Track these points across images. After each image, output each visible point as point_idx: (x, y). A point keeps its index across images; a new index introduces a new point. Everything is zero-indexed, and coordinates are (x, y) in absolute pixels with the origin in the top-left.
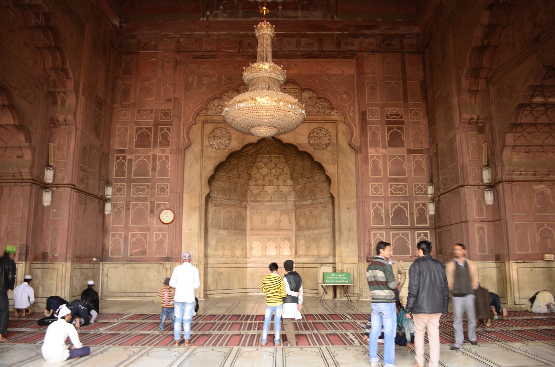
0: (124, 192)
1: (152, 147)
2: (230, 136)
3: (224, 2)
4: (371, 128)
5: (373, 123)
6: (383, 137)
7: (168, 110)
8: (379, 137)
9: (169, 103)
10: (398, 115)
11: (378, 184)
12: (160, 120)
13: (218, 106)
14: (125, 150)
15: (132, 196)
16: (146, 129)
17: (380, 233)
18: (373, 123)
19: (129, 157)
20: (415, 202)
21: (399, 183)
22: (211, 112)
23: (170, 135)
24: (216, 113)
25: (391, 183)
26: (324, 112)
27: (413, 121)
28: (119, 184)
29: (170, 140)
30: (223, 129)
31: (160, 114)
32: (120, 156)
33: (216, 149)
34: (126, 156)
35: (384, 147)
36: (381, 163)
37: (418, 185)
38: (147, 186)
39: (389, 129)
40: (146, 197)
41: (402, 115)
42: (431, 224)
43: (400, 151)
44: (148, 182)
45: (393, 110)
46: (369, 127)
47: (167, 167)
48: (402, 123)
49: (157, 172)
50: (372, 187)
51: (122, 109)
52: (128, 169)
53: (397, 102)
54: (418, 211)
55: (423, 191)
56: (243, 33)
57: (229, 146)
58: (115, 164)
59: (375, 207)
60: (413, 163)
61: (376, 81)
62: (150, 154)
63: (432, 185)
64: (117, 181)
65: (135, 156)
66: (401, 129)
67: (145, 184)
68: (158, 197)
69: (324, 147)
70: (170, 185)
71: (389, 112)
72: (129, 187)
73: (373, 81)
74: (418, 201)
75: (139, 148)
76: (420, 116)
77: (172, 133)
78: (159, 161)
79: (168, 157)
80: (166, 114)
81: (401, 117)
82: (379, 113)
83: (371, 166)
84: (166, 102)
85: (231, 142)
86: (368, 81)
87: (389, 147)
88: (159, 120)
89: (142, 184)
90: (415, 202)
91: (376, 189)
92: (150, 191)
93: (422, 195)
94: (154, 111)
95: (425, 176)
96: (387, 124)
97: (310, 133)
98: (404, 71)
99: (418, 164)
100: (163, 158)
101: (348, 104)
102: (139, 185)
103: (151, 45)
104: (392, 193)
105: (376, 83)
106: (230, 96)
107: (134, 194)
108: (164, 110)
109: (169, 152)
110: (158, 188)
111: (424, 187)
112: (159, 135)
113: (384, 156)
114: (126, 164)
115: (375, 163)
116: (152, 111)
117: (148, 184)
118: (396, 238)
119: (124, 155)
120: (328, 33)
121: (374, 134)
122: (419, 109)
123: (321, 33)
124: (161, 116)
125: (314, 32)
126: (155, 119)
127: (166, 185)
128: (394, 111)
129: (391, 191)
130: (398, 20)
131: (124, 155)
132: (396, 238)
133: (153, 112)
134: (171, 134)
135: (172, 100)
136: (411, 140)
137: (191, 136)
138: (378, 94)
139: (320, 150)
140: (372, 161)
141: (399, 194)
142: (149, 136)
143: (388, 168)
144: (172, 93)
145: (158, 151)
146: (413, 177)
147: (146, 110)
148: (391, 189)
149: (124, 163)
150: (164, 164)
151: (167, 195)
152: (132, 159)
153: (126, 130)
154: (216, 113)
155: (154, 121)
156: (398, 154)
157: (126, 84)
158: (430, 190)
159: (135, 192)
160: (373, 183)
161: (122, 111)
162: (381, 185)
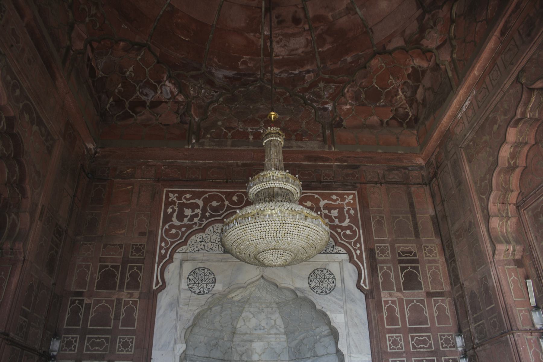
0: (75, 347)
1: (117, 289)
3: (212, 131)
4: (382, 268)
5: (384, 262)
6: (397, 277)
7: (140, 245)
8: (392, 278)
9: (142, 237)
11: (396, 336)
13: (201, 242)
14: (83, 292)
15: (84, 352)
16: (112, 266)
18: (384, 262)
19: (87, 301)
20: (443, 358)
21: (421, 334)
22: (192, 249)
23: (141, 275)
24: (198, 250)
25: (412, 334)
26: (325, 250)
27: (428, 259)
28: (70, 336)
29: (140, 282)
30: (206, 270)
31: (131, 250)
32: (76, 300)
34: (83, 300)
35: (399, 290)
36: (397, 309)
37: (444, 336)
38: (107, 339)
39: (403, 269)
40: (103, 354)
41: (415, 253)
43: (418, 295)
44: (108, 334)
45: (405, 247)
46: (380, 267)
47: (134, 315)
49: (121, 321)
50: (390, 341)
51: (85, 242)
52: (84, 316)
55: (451, 343)
56: (232, 162)
58: (68, 310)
60: (434, 309)
61: (383, 215)
62: (114, 298)
64: (68, 332)
65: (94, 300)
66: (416, 268)
67: (103, 336)
68: (119, 354)
69: (328, 292)
70: (136, 339)
71: (400, 249)
72: (82, 340)
73: (379, 215)
74: (448, 356)
75: (101, 290)
76: (436, 253)
77: (143, 273)
79: (137, 301)
80: (138, 250)
81: (415, 255)
82: (390, 251)
83: (386, 314)
84: (139, 235)
85: (214, 285)
86: (373, 215)
87: (404, 290)
89: (100, 336)
90: (443, 358)
91: (395, 343)
92: (109, 346)
93: (450, 349)
94: (124, 246)
95: (451, 324)
96: (400, 263)
97: (310, 275)
99: (440, 309)
101: (353, 240)
102: (96, 338)
103: (127, 173)
104: (414, 347)
105: (383, 217)
106: (215, 230)
107: (88, 350)
108: (136, 245)
109: (138, 297)
110: (120, 342)
111: (452, 338)
112: (128, 275)
113: (401, 301)
114: (83, 310)
115: (391, 310)
116: (121, 246)
117: (108, 336)
119: (81, 298)
120: (325, 163)
121: (386, 276)
122: (433, 245)
123: (318, 163)
124: (132, 252)
127: (131, 338)
128: (406, 248)
129: (413, 344)
130: (399, 152)
131: (81, 298)
134: (142, 274)
135: (146, 233)
137: (167, 276)
139: (323, 295)
140: (386, 308)
141: (423, 348)
142: (115, 276)
143: (407, 316)
144: (147, 225)
145: (124, 295)
146: (437, 325)
147: (114, 245)
148: (412, 342)
149: (81, 309)
150: (129, 311)
151: (131, 351)
152: (91, 304)
153: (88, 267)
154: (198, 250)
155: (123, 258)
156: (416, 299)
157: (94, 214)
158: (459, 341)
159: (90, 347)
160: (390, 335)
161: (85, 244)
162: (400, 336)
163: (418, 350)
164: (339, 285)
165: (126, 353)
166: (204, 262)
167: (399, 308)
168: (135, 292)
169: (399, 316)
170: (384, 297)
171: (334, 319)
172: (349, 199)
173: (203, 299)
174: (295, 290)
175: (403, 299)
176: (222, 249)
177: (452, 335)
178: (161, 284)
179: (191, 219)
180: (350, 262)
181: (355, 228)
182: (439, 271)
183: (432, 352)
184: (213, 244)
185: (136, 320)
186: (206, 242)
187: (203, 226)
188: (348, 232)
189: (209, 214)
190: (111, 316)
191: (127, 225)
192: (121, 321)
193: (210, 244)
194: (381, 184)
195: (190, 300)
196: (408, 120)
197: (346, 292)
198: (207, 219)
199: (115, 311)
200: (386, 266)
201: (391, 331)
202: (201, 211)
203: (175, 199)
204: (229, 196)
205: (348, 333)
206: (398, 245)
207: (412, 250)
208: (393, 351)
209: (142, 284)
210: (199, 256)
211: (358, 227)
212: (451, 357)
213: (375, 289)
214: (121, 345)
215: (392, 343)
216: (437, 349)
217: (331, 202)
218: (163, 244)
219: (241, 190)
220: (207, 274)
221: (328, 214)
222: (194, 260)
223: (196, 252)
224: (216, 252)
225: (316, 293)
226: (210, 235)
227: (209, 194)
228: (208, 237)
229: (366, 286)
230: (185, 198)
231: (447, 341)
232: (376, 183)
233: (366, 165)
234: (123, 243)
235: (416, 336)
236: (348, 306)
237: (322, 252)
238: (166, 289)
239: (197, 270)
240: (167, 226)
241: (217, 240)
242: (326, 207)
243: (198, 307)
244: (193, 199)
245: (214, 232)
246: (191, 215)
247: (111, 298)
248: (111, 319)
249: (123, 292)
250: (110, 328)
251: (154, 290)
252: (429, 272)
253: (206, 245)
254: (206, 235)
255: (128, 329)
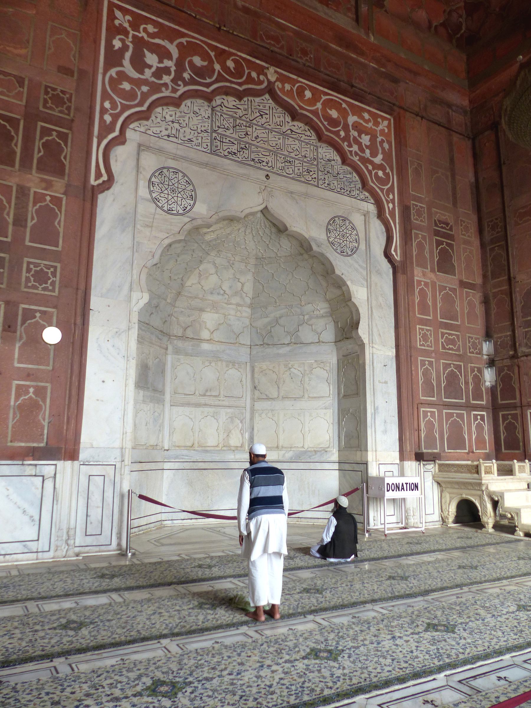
2: (194, 190)
4: (417, 235)
5: (419, 228)
6: (431, 252)
7: (63, 92)
9: (65, 76)
10: (447, 224)
12: (41, 108)
17: (431, 412)
18: (419, 228)
22: (158, 130)
23: (67, 151)
24: (169, 136)
25: (443, 331)
26: (350, 192)
29: (67, 163)
31: (42, 96)
33: (164, 211)
36: (430, 294)
39: (439, 243)
41: (451, 226)
42: (487, 401)
47: (56, 223)
48: (450, 237)
49: (28, 230)
53: (446, 204)
54: (472, 378)
57: (190, 210)
59: (425, 367)
60: (465, 303)
63: (490, 341)
68: (27, 292)
70: (62, 269)
76: (471, 232)
77: (72, 148)
78: (35, 204)
79: (60, 199)
80: (58, 100)
81: (451, 229)
85: (194, 204)
87: (438, 271)
88: (38, 108)
90: (469, 365)
91: (425, 337)
92: (6, 275)
93: (476, 355)
94: (26, 82)
95: (479, 325)
96: (436, 235)
97: (329, 223)
98: (452, 160)
100: (45, 200)
101: (386, 187)
106: (196, 109)
108: (54, 89)
109: (62, 190)
110: (29, 270)
111: (479, 342)
112: (38, 144)
116: (21, 81)
118: (450, 422)
123: (350, 54)
125: (340, 47)
126: (27, 102)
127: (52, 266)
129: (442, 343)
132: (450, 422)
133: (23, 83)
134: (69, 149)
136: (463, 267)
137: (115, 167)
138: (424, 184)
139: (343, 255)
144: (74, 56)
158: (487, 348)
160: (420, 327)
163: (447, 351)
164: (362, 246)
165: (43, 292)
166: (176, 160)
167: (432, 294)
168: (57, 181)
169: (430, 304)
170: (418, 276)
171: (355, 293)
172: (383, 125)
173: (178, 222)
174: (309, 240)
175: (436, 283)
176: (207, 145)
177: (478, 339)
178: (105, 177)
179: (159, 73)
180: (377, 218)
181: (388, 170)
182: (473, 257)
183: (459, 355)
184: (193, 132)
185: (61, 235)
186: (181, 125)
187: (179, 93)
188: (380, 173)
189: (189, 77)
190: (7, 217)
191: (31, 42)
192: (28, 230)
193: (188, 130)
194: (422, 118)
195: (155, 220)
196: (458, 36)
197: (372, 259)
198: (186, 84)
199: (15, 208)
200: (421, 235)
201: (423, 322)
202: (175, 65)
203: (126, 25)
204: (222, 55)
205: (371, 316)
206: (435, 210)
207: (449, 222)
208: (423, 348)
209: (70, 168)
210: (169, 146)
211: (392, 171)
212: (476, 366)
213: (408, 262)
214: (32, 275)
215: (422, 337)
216: (465, 353)
217: (362, 122)
218: (107, 105)
219: (239, 54)
220: (183, 182)
221: (358, 138)
222: (160, 151)
223: (164, 138)
224: (198, 148)
225: (336, 250)
226: (188, 115)
227: (188, 39)
228: (184, 117)
229: (397, 255)
230: (145, 30)
231: (474, 345)
232: (417, 115)
233: (407, 83)
234: (23, 76)
235: (447, 333)
236: (373, 278)
237: (345, 194)
238: (111, 190)
239: (165, 171)
240: (113, 72)
241: (199, 126)
242: (356, 126)
243: (168, 235)
244: (159, 38)
245: (195, 113)
246: (157, 67)
247: (5, 180)
248: (8, 223)
249: (30, 176)
250: (5, 239)
251: (93, 186)
252: (464, 255)
253: (182, 131)
254: (181, 112)
255: (45, 249)
